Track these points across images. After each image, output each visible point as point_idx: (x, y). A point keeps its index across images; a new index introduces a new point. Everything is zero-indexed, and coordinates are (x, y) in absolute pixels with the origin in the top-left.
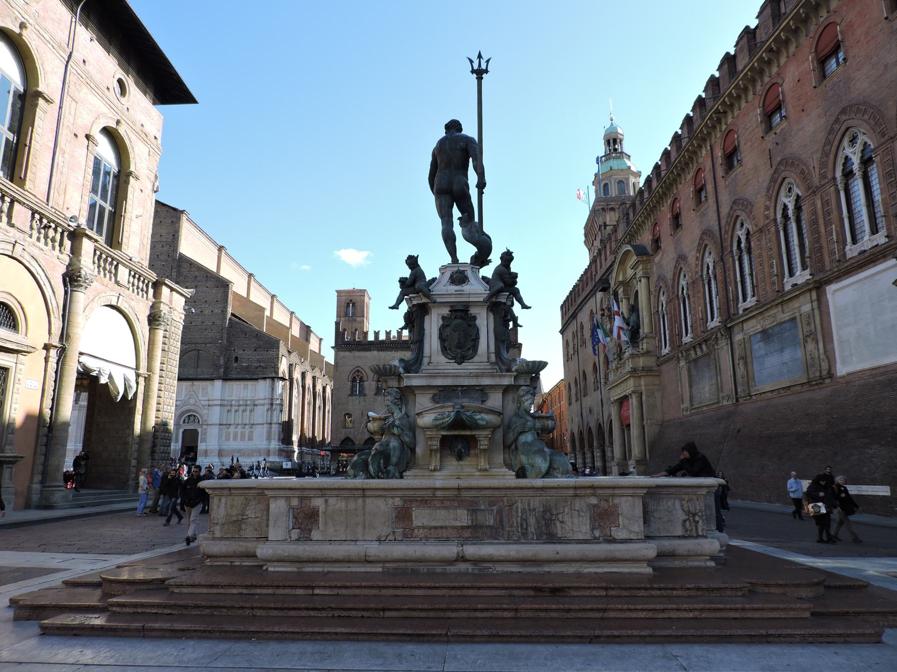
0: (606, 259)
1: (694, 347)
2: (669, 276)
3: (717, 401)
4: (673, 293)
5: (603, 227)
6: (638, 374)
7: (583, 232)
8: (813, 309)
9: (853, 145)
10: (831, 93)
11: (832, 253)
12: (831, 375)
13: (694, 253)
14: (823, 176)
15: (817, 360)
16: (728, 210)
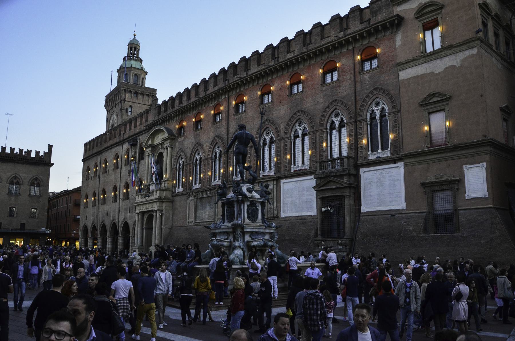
0: (135, 127)
1: (202, 192)
2: (188, 151)
3: (213, 220)
4: (190, 160)
5: (123, 101)
6: (162, 200)
7: (105, 99)
8: (274, 188)
9: (300, 126)
10: (294, 101)
11: (286, 166)
12: (278, 217)
13: (208, 144)
14: (286, 134)
15: (272, 210)
16: (234, 131)
